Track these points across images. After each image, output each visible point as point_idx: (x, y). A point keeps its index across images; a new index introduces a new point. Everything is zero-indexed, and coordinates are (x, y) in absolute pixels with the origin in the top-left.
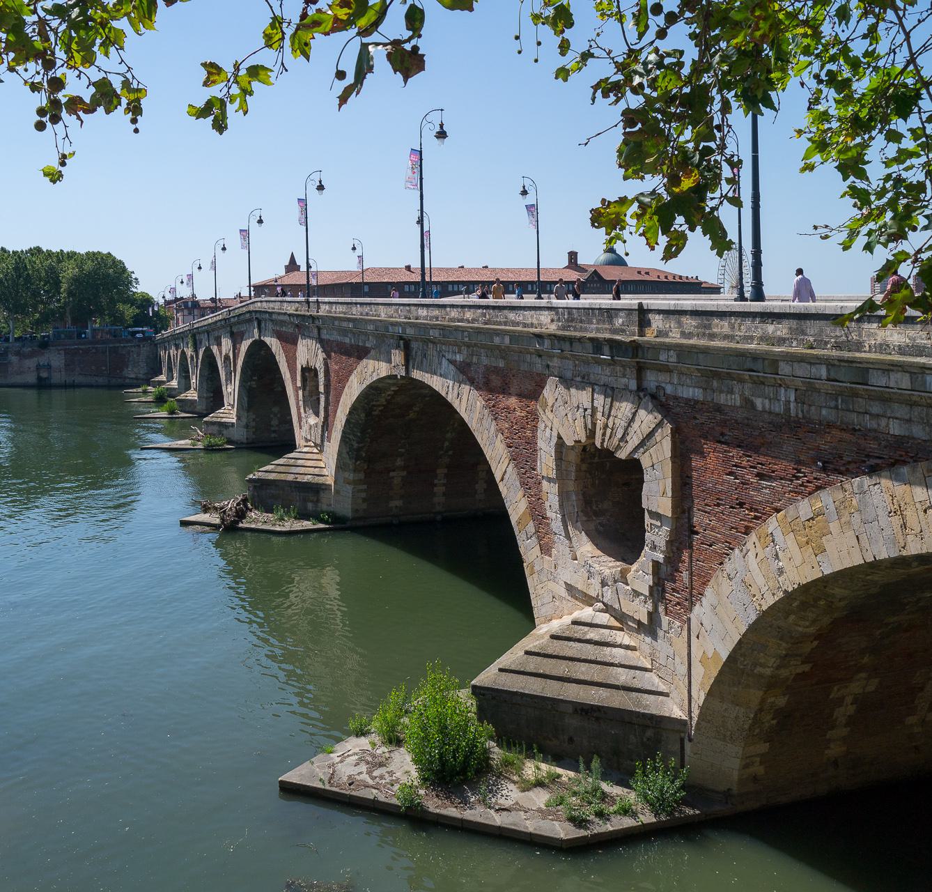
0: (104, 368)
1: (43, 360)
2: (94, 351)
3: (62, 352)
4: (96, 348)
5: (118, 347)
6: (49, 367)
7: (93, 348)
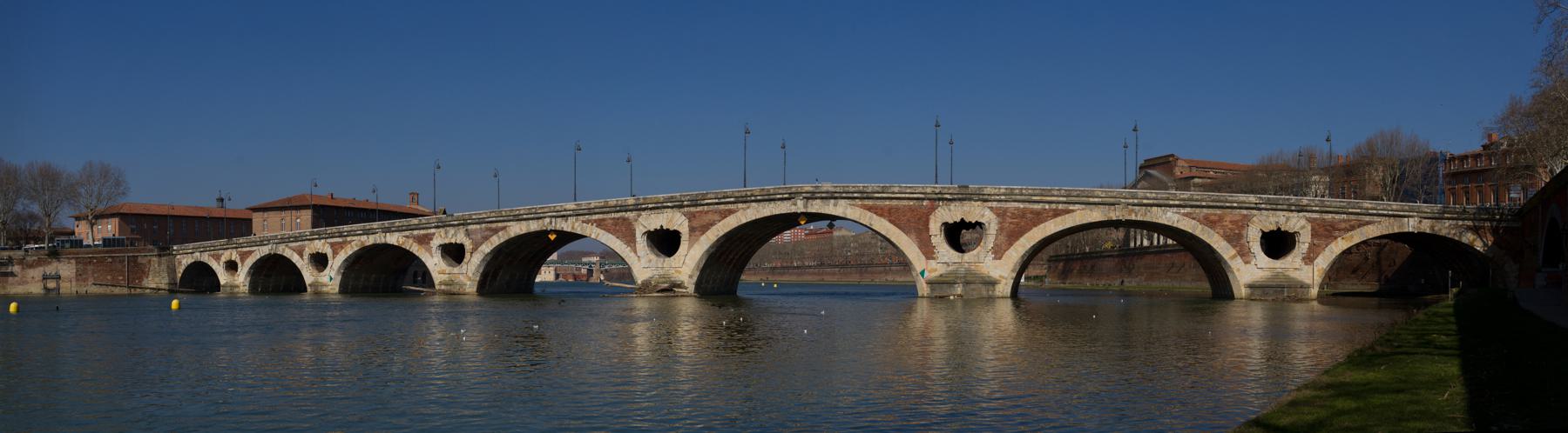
0: (121, 278)
1: (51, 269)
2: (110, 260)
3: (73, 261)
4: (112, 257)
5: (137, 256)
6: (58, 278)
7: (109, 257)
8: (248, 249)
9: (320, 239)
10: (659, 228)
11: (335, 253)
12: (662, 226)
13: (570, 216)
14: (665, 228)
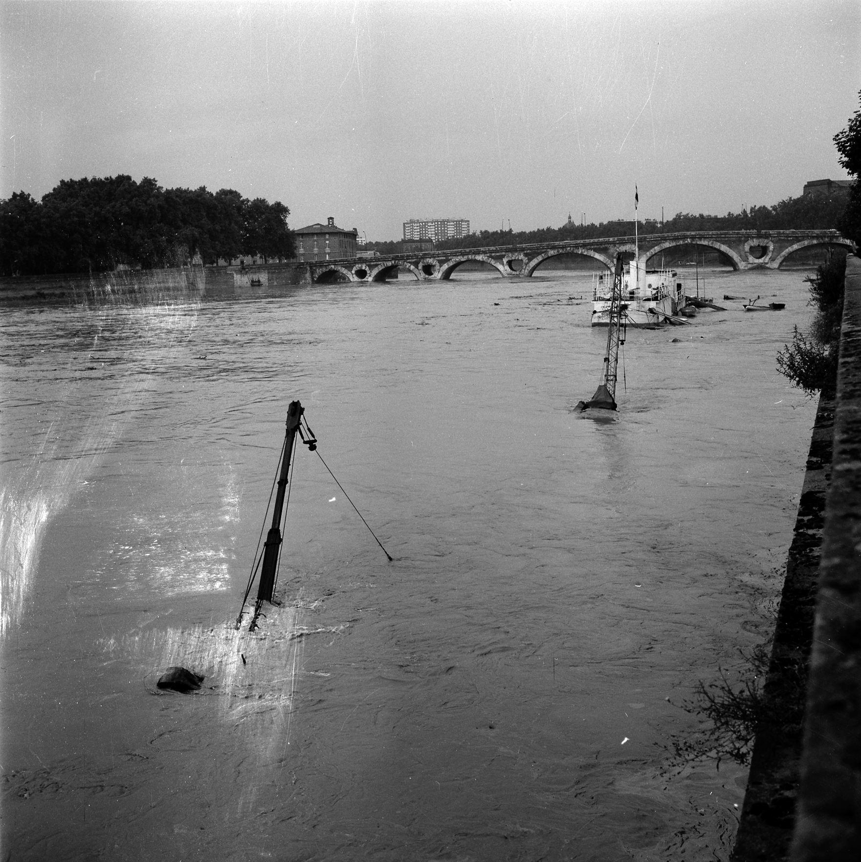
8: (375, 263)
9: (430, 258)
11: (441, 266)
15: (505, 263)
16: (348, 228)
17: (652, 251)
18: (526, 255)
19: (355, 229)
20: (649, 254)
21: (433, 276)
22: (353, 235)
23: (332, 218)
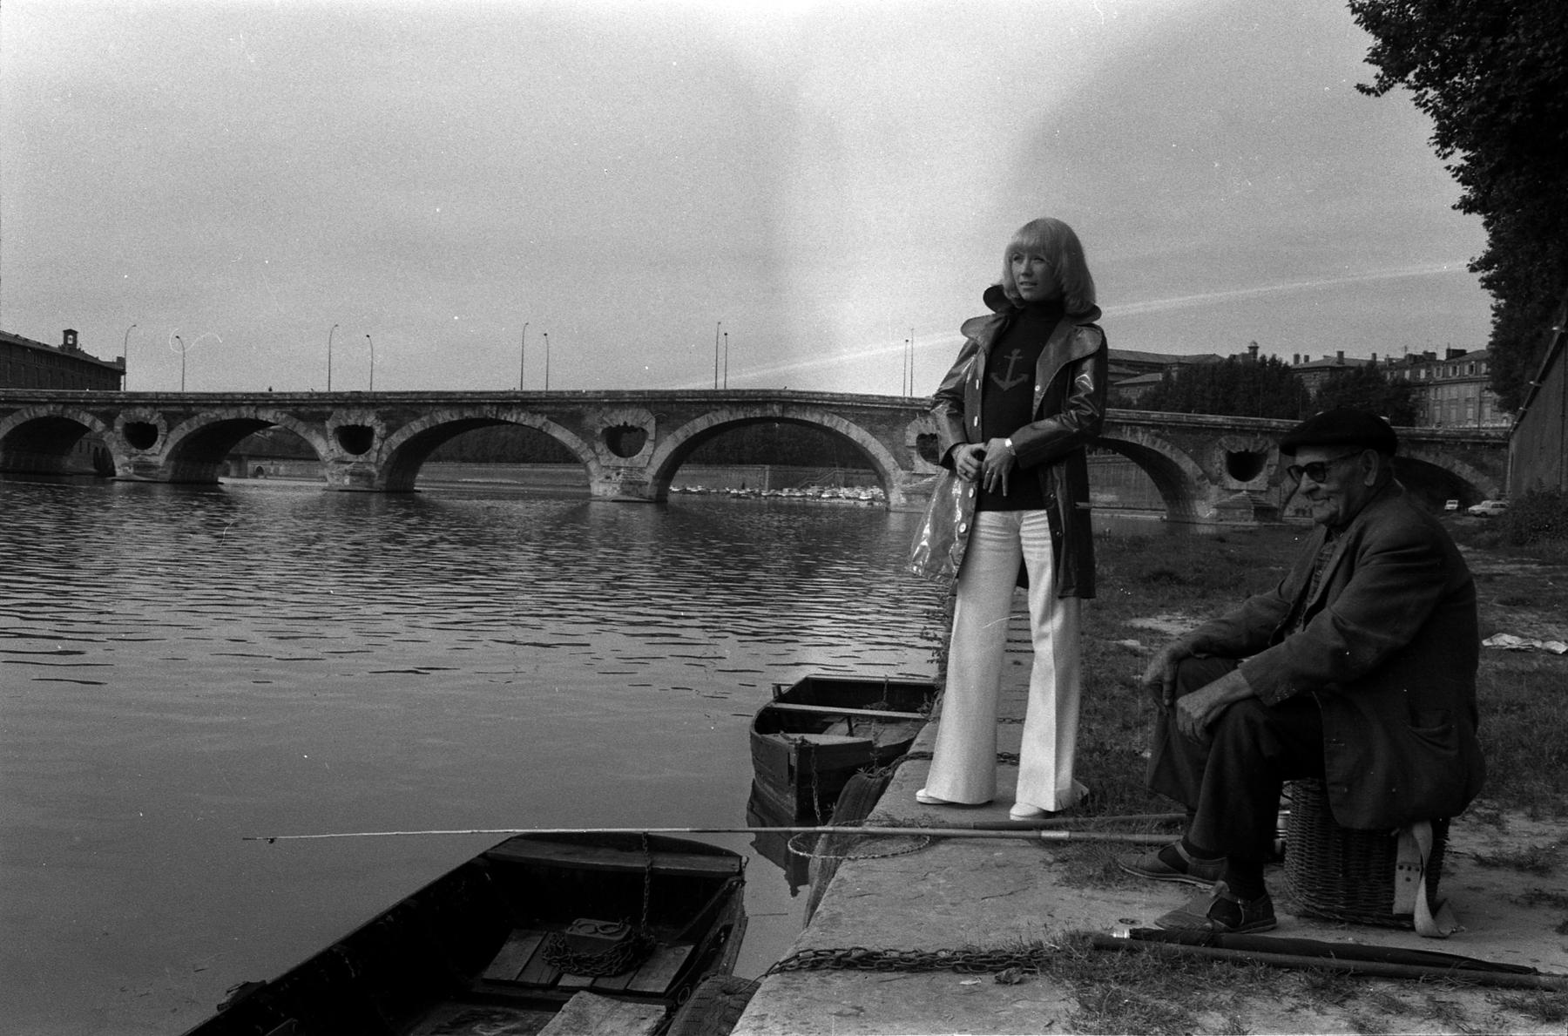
10: (622, 424)
11: (170, 429)
12: (625, 423)
13: (515, 404)
14: (629, 425)
15: (330, 433)
16: (106, 356)
17: (686, 426)
18: (383, 417)
19: (121, 361)
20: (681, 435)
21: (148, 451)
22: (114, 372)
23: (74, 333)
